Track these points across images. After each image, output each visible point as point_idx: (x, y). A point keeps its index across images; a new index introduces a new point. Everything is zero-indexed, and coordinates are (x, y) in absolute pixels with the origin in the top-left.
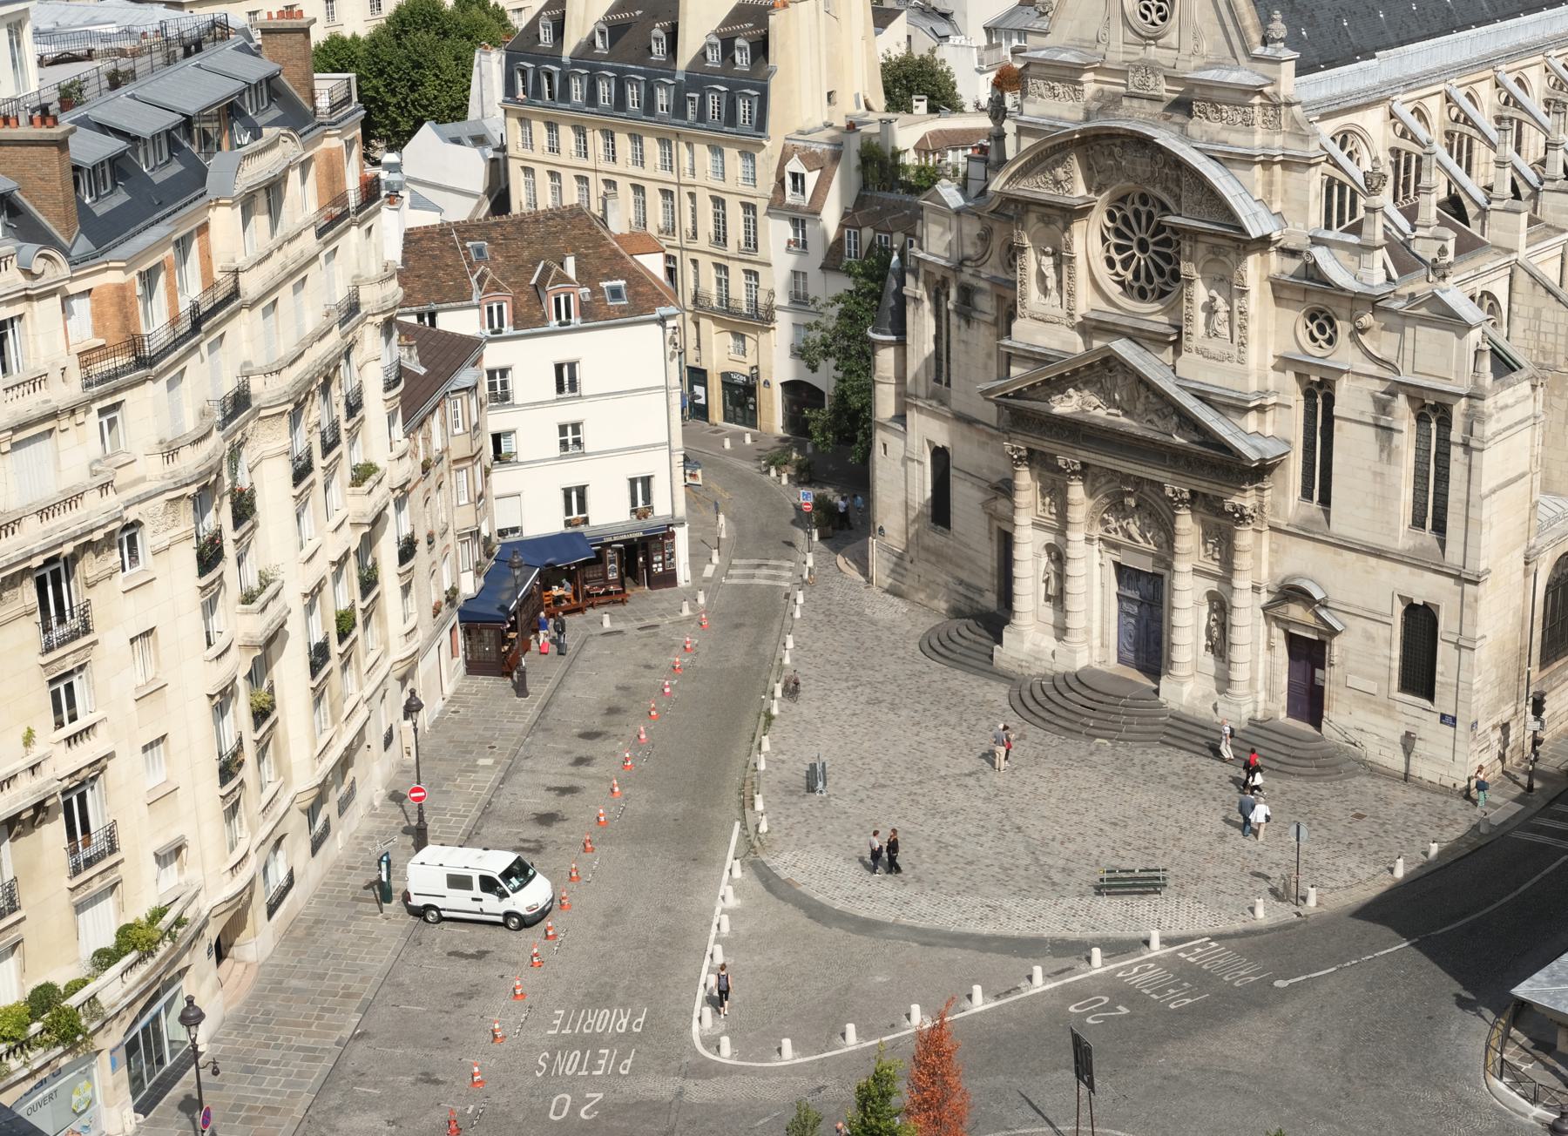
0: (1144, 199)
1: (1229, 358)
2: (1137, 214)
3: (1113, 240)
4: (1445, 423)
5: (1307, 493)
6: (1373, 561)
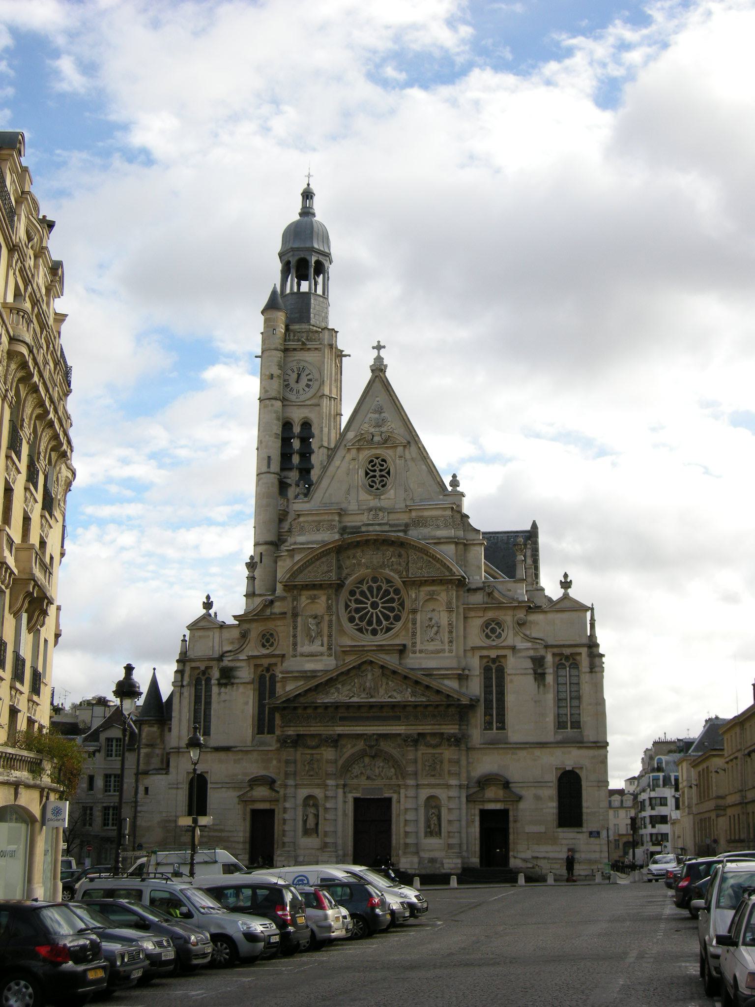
0: (375, 580)
1: (443, 651)
2: (370, 589)
3: (353, 605)
4: (575, 665)
5: (488, 726)
6: (537, 752)
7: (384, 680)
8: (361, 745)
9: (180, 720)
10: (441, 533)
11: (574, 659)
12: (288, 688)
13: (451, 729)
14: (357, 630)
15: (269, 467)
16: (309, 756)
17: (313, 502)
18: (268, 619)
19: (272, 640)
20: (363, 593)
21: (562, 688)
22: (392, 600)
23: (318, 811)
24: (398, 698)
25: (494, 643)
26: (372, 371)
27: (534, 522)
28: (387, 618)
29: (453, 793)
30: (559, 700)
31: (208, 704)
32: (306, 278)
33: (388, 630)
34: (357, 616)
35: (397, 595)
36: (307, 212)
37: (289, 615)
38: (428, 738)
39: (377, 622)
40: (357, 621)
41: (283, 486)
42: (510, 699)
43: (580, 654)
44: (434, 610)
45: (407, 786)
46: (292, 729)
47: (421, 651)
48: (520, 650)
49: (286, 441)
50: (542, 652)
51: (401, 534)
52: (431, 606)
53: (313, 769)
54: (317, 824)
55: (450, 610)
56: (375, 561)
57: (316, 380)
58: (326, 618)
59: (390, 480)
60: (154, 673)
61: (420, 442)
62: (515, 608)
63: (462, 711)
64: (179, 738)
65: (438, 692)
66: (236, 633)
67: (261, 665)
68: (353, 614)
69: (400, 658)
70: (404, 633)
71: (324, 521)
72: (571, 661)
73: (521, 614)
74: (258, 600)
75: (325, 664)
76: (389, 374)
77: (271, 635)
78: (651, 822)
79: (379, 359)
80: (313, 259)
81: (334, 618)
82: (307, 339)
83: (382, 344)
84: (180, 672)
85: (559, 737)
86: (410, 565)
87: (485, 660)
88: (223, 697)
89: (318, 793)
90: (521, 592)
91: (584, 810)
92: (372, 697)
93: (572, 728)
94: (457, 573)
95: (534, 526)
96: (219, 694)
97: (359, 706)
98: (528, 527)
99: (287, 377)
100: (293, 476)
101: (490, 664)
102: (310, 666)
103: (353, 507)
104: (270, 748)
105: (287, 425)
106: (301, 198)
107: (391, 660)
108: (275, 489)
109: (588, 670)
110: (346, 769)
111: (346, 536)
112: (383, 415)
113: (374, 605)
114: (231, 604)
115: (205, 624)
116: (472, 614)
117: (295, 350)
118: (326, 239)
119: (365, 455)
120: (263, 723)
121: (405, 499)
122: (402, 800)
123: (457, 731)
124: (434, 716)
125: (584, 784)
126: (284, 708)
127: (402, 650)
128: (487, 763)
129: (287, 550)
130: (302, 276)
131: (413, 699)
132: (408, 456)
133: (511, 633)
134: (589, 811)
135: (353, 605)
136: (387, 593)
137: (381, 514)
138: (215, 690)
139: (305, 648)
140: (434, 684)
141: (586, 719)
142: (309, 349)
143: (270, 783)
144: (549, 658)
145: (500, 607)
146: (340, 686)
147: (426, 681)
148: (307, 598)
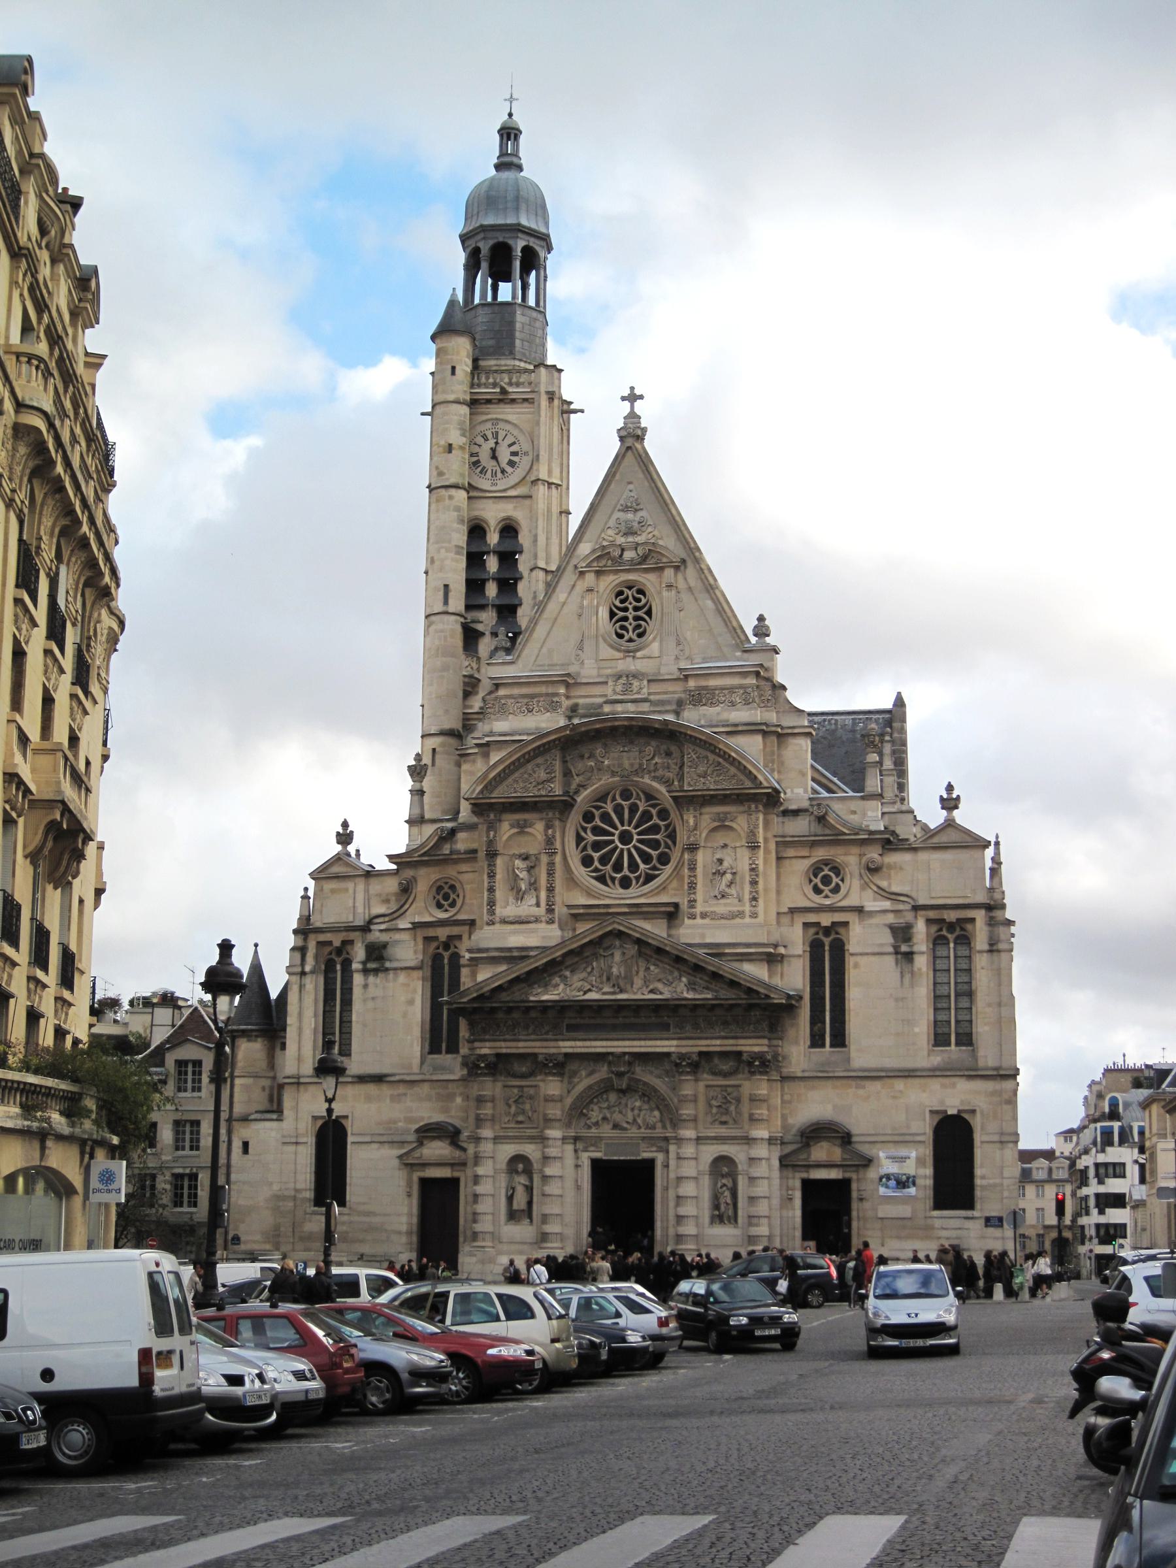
1: (741, 914)
2: (618, 810)
3: (591, 838)
4: (965, 940)
5: (817, 1041)
6: (899, 1084)
7: (642, 964)
8: (603, 1072)
9: (300, 1029)
10: (740, 715)
11: (962, 929)
12: (480, 977)
13: (753, 1046)
14: (596, 878)
15: (446, 602)
16: (516, 1091)
17: (520, 663)
18: (446, 861)
19: (452, 896)
20: (605, 817)
21: (942, 978)
22: (655, 829)
23: (531, 1180)
24: (666, 993)
25: (827, 902)
26: (622, 439)
27: (899, 693)
28: (647, 859)
29: (761, 1151)
30: (939, 1000)
31: (347, 1003)
32: (507, 278)
33: (649, 878)
34: (596, 855)
35: (663, 820)
36: (507, 163)
37: (481, 854)
38: (716, 1061)
39: (630, 866)
40: (596, 863)
41: (471, 636)
42: (854, 995)
43: (973, 920)
44: (725, 846)
45: (679, 1141)
46: (488, 1044)
47: (704, 915)
48: (871, 914)
49: (475, 560)
50: (909, 917)
51: (670, 717)
52: (721, 838)
53: (523, 1112)
54: (530, 1203)
55: (753, 847)
56: (626, 764)
57: (526, 454)
58: (544, 859)
59: (652, 627)
60: (256, 952)
61: (704, 560)
62: (863, 842)
63: (771, 1013)
64: (299, 1059)
65: (733, 984)
66: (392, 885)
67: (436, 938)
68: (590, 852)
69: (669, 927)
70: (675, 884)
71: (541, 695)
72: (833, 936)
73: (873, 854)
74: (429, 830)
75: (543, 936)
76: (651, 445)
77: (453, 887)
78: (1097, 1206)
79: (633, 416)
80: (519, 245)
81: (558, 859)
82: (510, 384)
83: (637, 392)
84: (300, 950)
85: (937, 1060)
86: (686, 769)
87: (812, 931)
88: (372, 991)
89: (531, 1150)
90: (873, 817)
91: (978, 1182)
92: (621, 991)
93: (957, 1044)
94: (765, 784)
95: (900, 702)
96: (366, 986)
97: (598, 1008)
98: (888, 704)
99: (476, 449)
100: (487, 619)
101: (821, 936)
102: (516, 939)
103: (589, 671)
104: (452, 1077)
105: (477, 531)
106: (497, 137)
107: (656, 929)
108: (458, 641)
109: (986, 947)
110: (578, 1111)
111: (576, 721)
112: (640, 514)
113: (625, 838)
114: (384, 838)
115: (339, 871)
116: (791, 852)
117: (489, 401)
118: (540, 208)
119: (609, 583)
120: (439, 1038)
121: (677, 658)
122: (672, 1163)
123: (765, 1049)
124: (726, 1023)
125: (978, 1137)
126: (475, 1011)
127: (672, 914)
128: (816, 1105)
129: (477, 745)
130: (500, 274)
131: (690, 995)
132: (681, 584)
133: (856, 883)
134: (984, 1182)
135: (591, 838)
136: (647, 816)
137: (636, 683)
138: (358, 979)
139: (508, 908)
140: (728, 968)
141: (982, 1029)
142: (513, 401)
143: (451, 1135)
144: (920, 928)
145: (837, 839)
146: (568, 973)
147: (713, 964)
148: (512, 826)
